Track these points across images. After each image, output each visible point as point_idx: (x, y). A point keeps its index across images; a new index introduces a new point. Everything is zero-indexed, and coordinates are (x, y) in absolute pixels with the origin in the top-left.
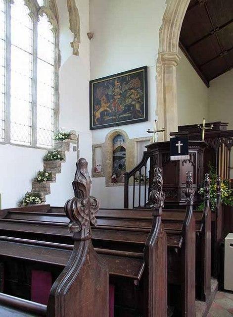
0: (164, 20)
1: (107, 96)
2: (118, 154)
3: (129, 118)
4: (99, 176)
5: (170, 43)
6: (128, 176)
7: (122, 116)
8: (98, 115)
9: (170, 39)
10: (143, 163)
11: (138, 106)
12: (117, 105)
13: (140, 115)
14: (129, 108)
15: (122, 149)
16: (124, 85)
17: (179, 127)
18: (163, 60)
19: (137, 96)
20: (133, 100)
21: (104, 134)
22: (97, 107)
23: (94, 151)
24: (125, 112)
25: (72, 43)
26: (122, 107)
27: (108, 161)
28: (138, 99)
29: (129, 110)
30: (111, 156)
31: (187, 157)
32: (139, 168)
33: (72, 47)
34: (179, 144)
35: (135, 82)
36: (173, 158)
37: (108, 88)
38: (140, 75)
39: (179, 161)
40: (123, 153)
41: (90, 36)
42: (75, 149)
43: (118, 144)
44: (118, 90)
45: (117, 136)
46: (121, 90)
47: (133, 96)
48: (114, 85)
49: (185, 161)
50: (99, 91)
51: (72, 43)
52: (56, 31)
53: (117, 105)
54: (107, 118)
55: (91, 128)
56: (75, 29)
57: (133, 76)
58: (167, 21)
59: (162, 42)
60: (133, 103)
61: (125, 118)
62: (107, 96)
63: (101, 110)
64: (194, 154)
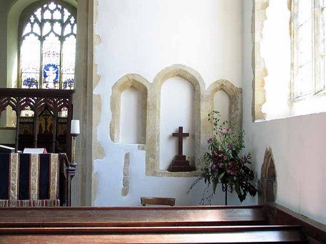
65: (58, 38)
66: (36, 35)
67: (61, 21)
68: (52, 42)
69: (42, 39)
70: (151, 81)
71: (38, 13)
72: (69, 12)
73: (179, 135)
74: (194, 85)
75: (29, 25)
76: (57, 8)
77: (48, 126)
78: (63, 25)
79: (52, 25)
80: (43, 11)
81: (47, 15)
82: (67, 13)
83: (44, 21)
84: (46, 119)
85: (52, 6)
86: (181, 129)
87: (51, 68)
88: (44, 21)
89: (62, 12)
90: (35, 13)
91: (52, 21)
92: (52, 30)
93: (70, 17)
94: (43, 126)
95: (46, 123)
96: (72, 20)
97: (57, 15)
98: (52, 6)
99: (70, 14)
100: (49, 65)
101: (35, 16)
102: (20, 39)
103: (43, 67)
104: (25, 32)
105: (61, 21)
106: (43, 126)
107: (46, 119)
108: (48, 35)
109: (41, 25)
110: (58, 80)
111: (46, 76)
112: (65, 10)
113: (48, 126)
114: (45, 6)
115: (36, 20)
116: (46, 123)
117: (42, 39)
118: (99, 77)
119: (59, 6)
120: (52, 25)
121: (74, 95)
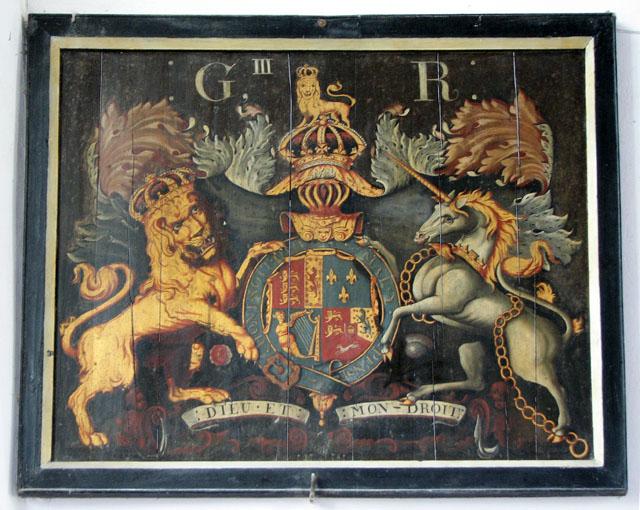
1: (211, 194)
7: (368, 410)
8: (108, 359)
11: (527, 352)
12: (314, 300)
16: (388, 133)
19: (519, 249)
20: (480, 286)
22: (98, 282)
24: (397, 375)
28: (530, 283)
29: (437, 367)
35: (511, 132)
44: (323, 168)
46: (363, 167)
47: (476, 246)
48: (280, 105)
50: (121, 137)
53: (314, 300)
54: (210, 407)
57: (481, 79)
60: (485, 310)
61: (408, 434)
62: (211, 194)
63: (149, 316)
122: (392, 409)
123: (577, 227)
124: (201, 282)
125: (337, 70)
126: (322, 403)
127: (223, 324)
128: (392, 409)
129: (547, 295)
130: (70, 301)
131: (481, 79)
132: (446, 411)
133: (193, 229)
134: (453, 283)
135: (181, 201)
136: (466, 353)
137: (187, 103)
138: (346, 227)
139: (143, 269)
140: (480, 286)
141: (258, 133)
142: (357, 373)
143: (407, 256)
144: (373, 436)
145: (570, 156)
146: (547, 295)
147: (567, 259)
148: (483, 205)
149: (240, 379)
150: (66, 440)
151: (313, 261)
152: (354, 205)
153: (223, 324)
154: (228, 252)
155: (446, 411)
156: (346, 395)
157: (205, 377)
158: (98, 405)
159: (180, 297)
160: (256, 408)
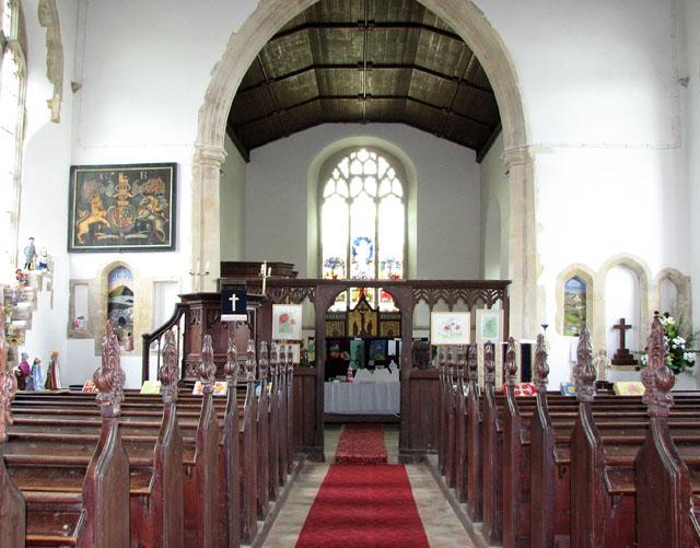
0: (207, 98)
1: (103, 198)
2: (119, 300)
3: (143, 241)
4: (82, 336)
5: (213, 133)
6: (148, 339)
7: (129, 236)
8: (84, 228)
9: (214, 126)
10: (174, 321)
11: (159, 225)
12: (121, 216)
13: (160, 237)
14: (141, 226)
15: (126, 291)
16: (135, 185)
17: (222, 263)
18: (202, 159)
19: (158, 206)
20: (151, 213)
21: (92, 265)
22: (83, 214)
23: (72, 290)
24: (135, 230)
25: (49, 101)
26: (130, 221)
27: (100, 311)
28: (160, 212)
29: (143, 228)
30: (106, 303)
31: (243, 318)
32: (169, 326)
33: (50, 107)
34: (234, 299)
35: (155, 184)
36: (224, 317)
37: (105, 184)
38: (164, 175)
39: (231, 322)
40: (128, 298)
41: (75, 87)
42: (49, 288)
43: (119, 282)
44: (123, 192)
45: (114, 271)
46: (130, 192)
47: (150, 206)
48: (116, 182)
49: (239, 323)
50: (88, 187)
51: (49, 101)
52: (23, 74)
53: (121, 216)
54: (103, 236)
55: (70, 250)
56: (54, 75)
57: (151, 175)
58: (212, 100)
59: (202, 130)
60: (151, 217)
61: (136, 241)
62: (103, 198)
63: (91, 220)
64: (252, 313)
65: (372, 200)
66: (341, 196)
67: (376, 176)
68: (364, 204)
69: (349, 201)
70: (596, 271)
71: (343, 164)
72: (387, 160)
73: (622, 327)
74: (638, 273)
75: (331, 183)
76: (370, 158)
77: (366, 324)
78: (379, 182)
79: (363, 181)
80: (351, 161)
81: (356, 168)
82: (384, 163)
83: (351, 176)
84: (363, 315)
85: (363, 154)
86: (623, 321)
87: (363, 242)
88: (351, 176)
89: (377, 162)
90: (340, 165)
91: (363, 177)
92: (363, 189)
93: (388, 170)
94: (359, 324)
95: (363, 321)
96: (392, 173)
97: (370, 168)
98: (363, 154)
99: (387, 165)
100: (361, 239)
101: (339, 170)
102: (320, 200)
103: (352, 241)
104: (326, 194)
105: (376, 176)
106: (359, 324)
107: (363, 315)
108: (357, 196)
109: (348, 181)
110: (373, 259)
111: (355, 254)
112: (382, 160)
113: (366, 324)
114: (353, 155)
115: (341, 176)
116: (363, 321)
117: (349, 201)
118: (542, 267)
119: (374, 155)
120: (363, 181)
121: (510, 288)
122: (134, 236)
123: (168, 202)
124: (101, 213)
125: (126, 173)
126: (122, 235)
127: (105, 221)
128: (134, 236)
129: (163, 214)
130: (77, 217)
131: (151, 175)
132: (144, 236)
133: (100, 204)
134: (146, 212)
135: (98, 199)
136: (148, 225)
137: (98, 180)
138: (127, 203)
139: (90, 211)
140: (151, 213)
141: (111, 186)
142: (128, 229)
143: (137, 207)
144: (131, 241)
145: (168, 189)
146: (163, 214)
147: (307, 299)
148: (152, 198)
149: (108, 231)
150: (76, 243)
151: (121, 209)
152: (128, 199)
153: (105, 221)
154: (106, 207)
155: (144, 236)
156: (126, 234)
157: (101, 231)
158: (83, 236)
159: (97, 216)
160: (110, 236)
